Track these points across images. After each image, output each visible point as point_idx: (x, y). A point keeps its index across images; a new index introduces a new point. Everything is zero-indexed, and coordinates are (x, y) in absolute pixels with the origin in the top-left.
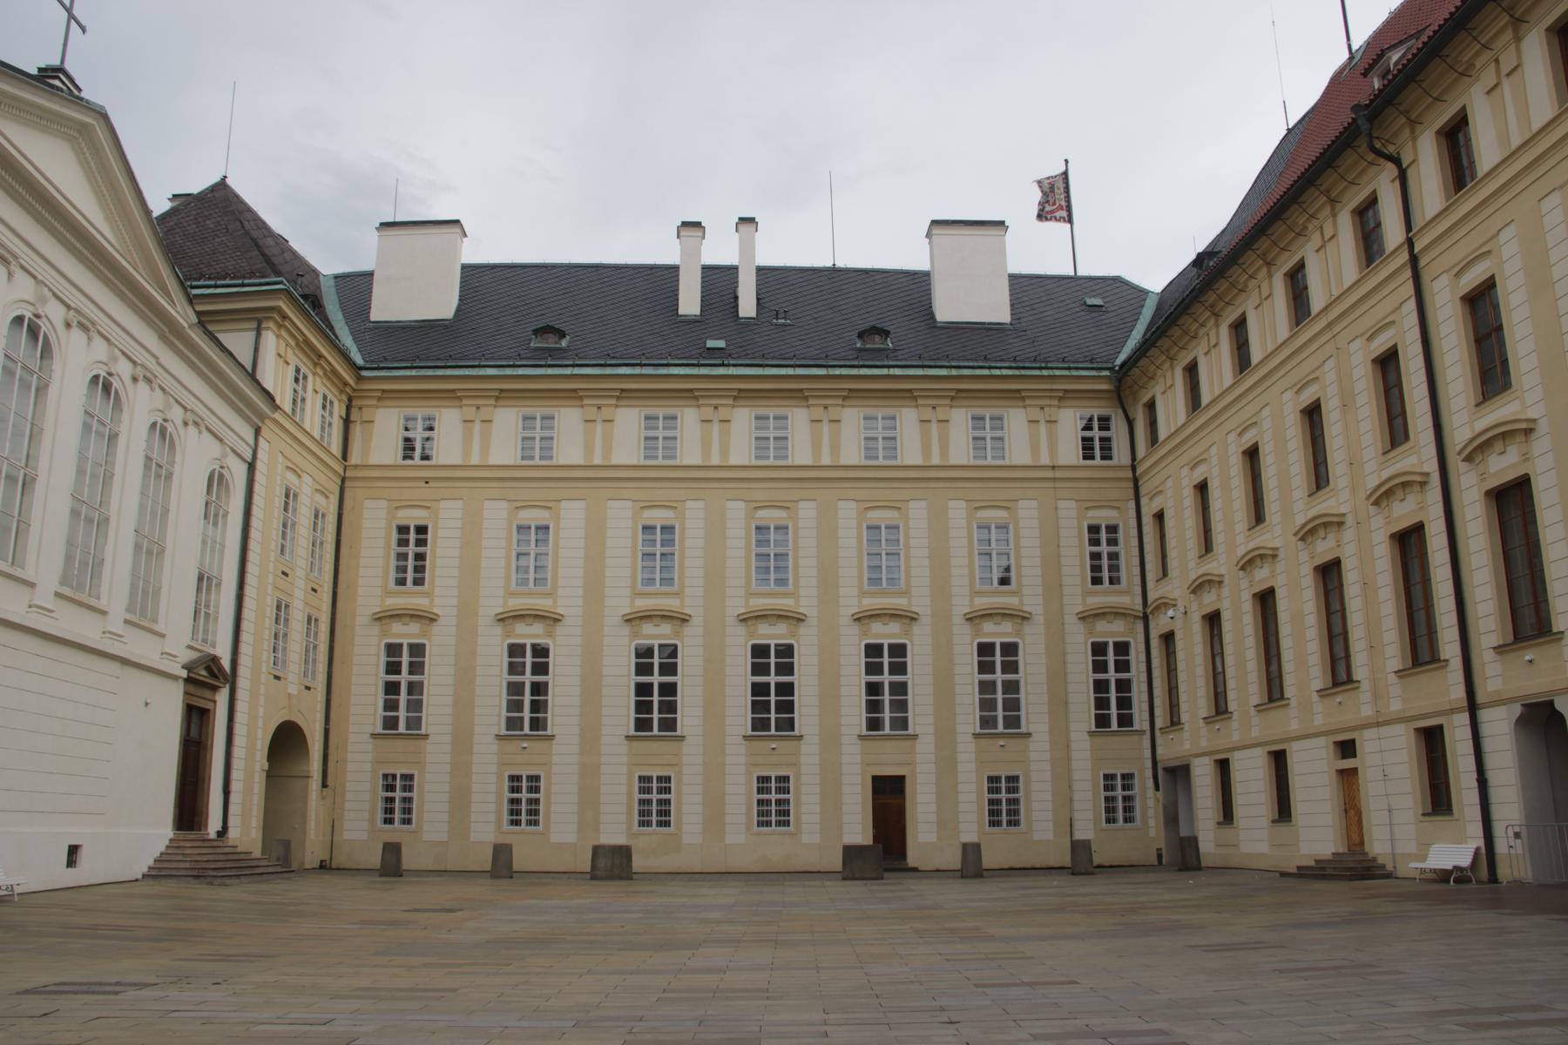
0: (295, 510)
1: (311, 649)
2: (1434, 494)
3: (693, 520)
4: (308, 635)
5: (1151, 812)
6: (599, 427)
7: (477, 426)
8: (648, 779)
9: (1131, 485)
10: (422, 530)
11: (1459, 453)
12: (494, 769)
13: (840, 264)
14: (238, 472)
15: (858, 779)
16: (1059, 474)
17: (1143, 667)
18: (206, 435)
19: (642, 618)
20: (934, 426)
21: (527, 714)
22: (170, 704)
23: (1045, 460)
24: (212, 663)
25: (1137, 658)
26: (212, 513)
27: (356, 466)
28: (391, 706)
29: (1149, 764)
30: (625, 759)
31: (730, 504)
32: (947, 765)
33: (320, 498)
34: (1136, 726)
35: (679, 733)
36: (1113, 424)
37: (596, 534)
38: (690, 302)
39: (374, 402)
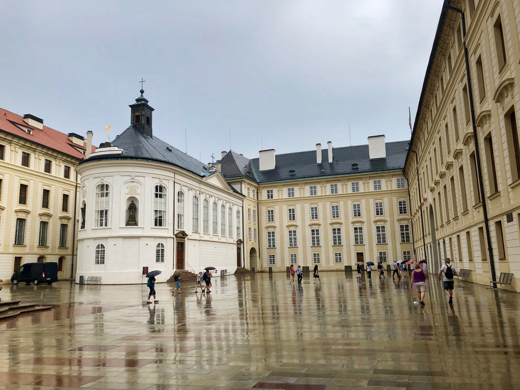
1: (255, 234)
3: (320, 206)
6: (302, 190)
7: (280, 191)
9: (408, 192)
10: (272, 211)
12: (288, 253)
13: (352, 145)
14: (241, 208)
16: (392, 192)
17: (411, 230)
21: (293, 243)
22: (235, 247)
23: (390, 189)
24: (240, 240)
26: (238, 217)
28: (269, 243)
30: (311, 251)
31: (327, 202)
32: (371, 250)
33: (254, 208)
37: (303, 210)
38: (319, 161)
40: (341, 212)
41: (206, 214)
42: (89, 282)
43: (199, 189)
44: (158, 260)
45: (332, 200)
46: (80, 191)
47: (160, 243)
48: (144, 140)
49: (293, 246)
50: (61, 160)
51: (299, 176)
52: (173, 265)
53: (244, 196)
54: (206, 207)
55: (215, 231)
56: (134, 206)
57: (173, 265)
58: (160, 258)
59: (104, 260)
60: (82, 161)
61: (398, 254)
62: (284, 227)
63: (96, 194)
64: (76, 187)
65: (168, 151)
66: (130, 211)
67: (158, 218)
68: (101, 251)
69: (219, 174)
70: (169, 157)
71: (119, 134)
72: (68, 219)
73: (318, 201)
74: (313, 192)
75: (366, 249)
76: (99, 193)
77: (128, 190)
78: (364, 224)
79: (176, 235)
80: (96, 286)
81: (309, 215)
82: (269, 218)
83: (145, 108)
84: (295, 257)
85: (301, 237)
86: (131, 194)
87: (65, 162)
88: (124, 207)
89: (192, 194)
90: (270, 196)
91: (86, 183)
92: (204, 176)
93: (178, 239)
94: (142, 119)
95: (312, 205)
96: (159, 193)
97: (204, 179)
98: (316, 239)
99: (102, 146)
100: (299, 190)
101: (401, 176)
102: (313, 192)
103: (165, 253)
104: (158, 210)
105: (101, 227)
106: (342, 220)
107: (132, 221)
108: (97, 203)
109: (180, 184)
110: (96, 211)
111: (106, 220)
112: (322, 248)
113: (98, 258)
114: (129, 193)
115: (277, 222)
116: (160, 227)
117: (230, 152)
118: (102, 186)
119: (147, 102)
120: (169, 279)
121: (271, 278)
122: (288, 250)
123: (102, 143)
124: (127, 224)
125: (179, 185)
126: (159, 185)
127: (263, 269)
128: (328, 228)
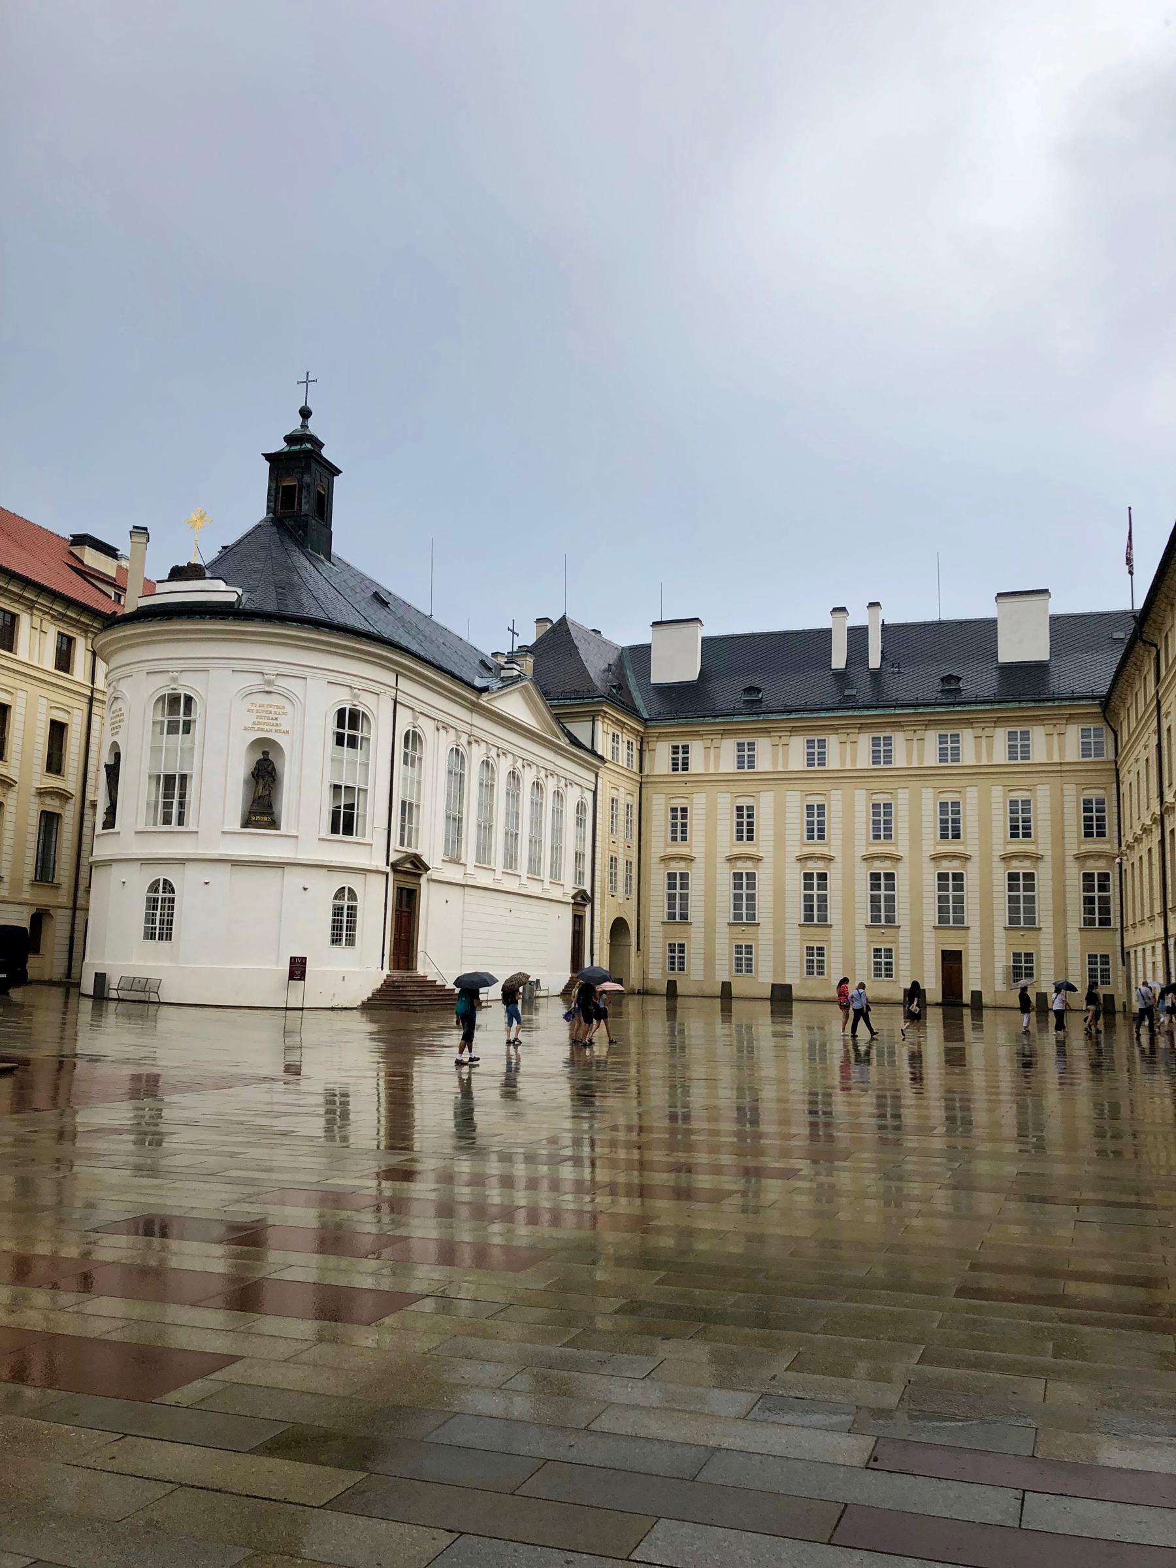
0: (617, 808)
1: (628, 878)
4: (627, 872)
8: (812, 948)
10: (684, 810)
13: (944, 618)
14: (589, 796)
15: (933, 952)
16: (1065, 768)
17: (1118, 889)
18: (574, 785)
19: (806, 858)
22: (567, 914)
23: (1056, 759)
25: (1114, 882)
26: (580, 822)
27: (647, 776)
28: (671, 906)
29: (1119, 949)
30: (799, 937)
31: (857, 792)
32: (987, 945)
33: (629, 797)
35: (828, 923)
38: (839, 660)
39: (655, 739)
41: (487, 807)
42: (122, 994)
43: (467, 728)
44: (335, 940)
45: (875, 785)
46: (105, 713)
47: (344, 888)
48: (307, 564)
50: (47, 613)
51: (775, 705)
52: (383, 955)
53: (601, 758)
54: (487, 786)
55: (511, 860)
56: (270, 769)
57: (383, 955)
58: (344, 933)
59: (171, 929)
60: (111, 621)
61: (1070, 961)
62: (718, 860)
63: (154, 722)
64: (91, 699)
65: (377, 606)
66: (257, 783)
67: (342, 810)
68: (163, 900)
69: (531, 687)
70: (381, 623)
71: (229, 542)
72: (63, 796)
73: (828, 786)
74: (816, 757)
75: (970, 941)
76: (162, 722)
77: (253, 717)
78: (969, 864)
79: (395, 867)
80: (141, 1006)
81: (798, 826)
82: (674, 832)
83: (314, 466)
85: (771, 893)
86: (262, 730)
87: (60, 620)
88: (240, 768)
89: (446, 741)
90: (680, 761)
91: (124, 687)
92: (485, 689)
93: (400, 877)
94: (303, 501)
95: (809, 798)
96: (347, 731)
97: (485, 697)
99: (178, 574)
100: (771, 748)
101: (1096, 720)
102: (816, 756)
103: (358, 919)
104: (344, 783)
105: (166, 828)
106: (900, 848)
107: (262, 814)
108: (155, 750)
109: (412, 709)
110: (150, 777)
111: (182, 805)
112: (833, 931)
113: (153, 922)
114: (256, 727)
115: (696, 845)
116: (348, 838)
117: (563, 620)
118: (174, 700)
119: (321, 445)
120: (369, 999)
121: (672, 1012)
123: (177, 566)
124: (246, 823)
125: (410, 712)
126: (348, 707)
127: (649, 985)
128: (857, 871)
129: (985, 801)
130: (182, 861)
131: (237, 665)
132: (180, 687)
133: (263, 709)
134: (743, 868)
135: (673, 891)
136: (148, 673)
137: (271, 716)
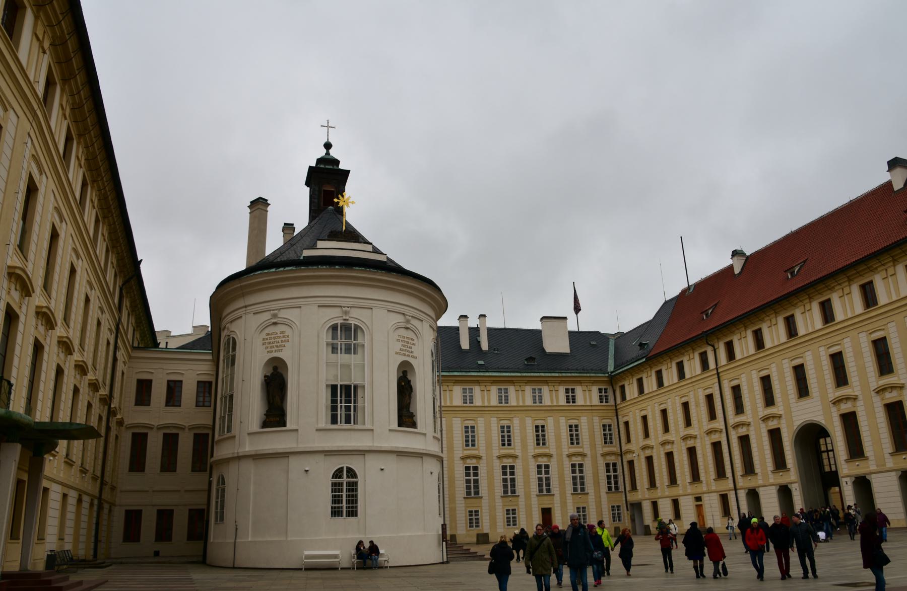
2: (724, 435)
3: (481, 424)
5: (626, 518)
8: (472, 511)
9: (615, 411)
11: (731, 426)
13: (507, 327)
15: (537, 509)
17: (621, 471)
20: (554, 392)
23: (588, 403)
29: (624, 502)
30: (464, 505)
31: (492, 419)
32: (564, 504)
34: (620, 490)
35: (480, 496)
36: (608, 390)
38: (465, 344)
40: (516, 438)
45: (501, 415)
49: (473, 495)
63: (327, 344)
75: (555, 501)
77: (398, 346)
81: (461, 439)
84: (513, 514)
86: (405, 355)
95: (466, 422)
98: (472, 484)
105: (347, 426)
106: (517, 451)
110: (327, 386)
122: (463, 502)
129: (557, 424)
130: (363, 453)
131: (391, 307)
132: (350, 319)
133: (404, 339)
134: (471, 464)
135: (547, 476)
136: (319, 306)
137: (409, 345)
